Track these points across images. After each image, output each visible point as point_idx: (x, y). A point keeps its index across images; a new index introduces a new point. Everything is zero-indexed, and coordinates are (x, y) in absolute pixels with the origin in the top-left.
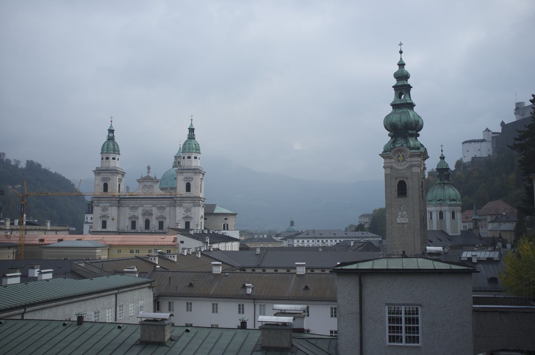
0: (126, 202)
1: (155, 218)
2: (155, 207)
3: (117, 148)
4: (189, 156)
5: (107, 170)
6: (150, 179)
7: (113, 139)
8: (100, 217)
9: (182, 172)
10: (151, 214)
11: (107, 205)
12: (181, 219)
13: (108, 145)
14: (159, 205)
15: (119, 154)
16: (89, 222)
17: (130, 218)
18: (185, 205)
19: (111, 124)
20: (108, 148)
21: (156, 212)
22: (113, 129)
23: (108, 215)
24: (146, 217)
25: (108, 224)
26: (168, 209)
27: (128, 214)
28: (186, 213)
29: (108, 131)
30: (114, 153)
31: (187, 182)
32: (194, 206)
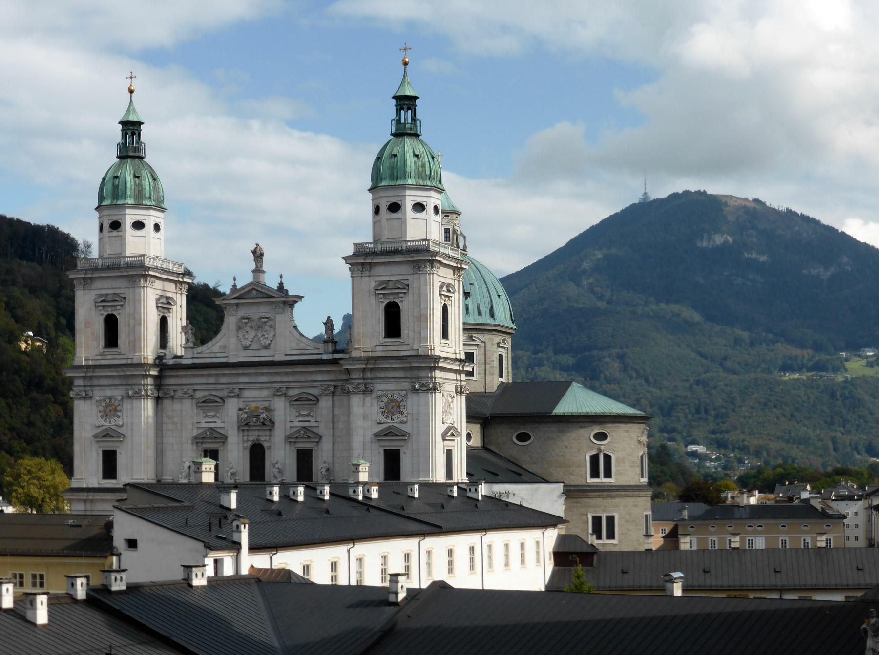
0: (184, 381)
1: (283, 437)
2: (283, 399)
3: (148, 188)
4: (394, 200)
6: (259, 295)
7: (137, 154)
8: (95, 436)
9: (370, 264)
10: (268, 424)
12: (368, 439)
14: (296, 391)
15: (163, 210)
19: (131, 101)
20: (116, 187)
21: (285, 415)
22: (136, 120)
23: (120, 430)
24: (253, 436)
25: (121, 461)
26: (325, 403)
27: (190, 427)
28: (387, 417)
29: (120, 126)
30: (138, 206)
31: (387, 301)
32: (414, 390)
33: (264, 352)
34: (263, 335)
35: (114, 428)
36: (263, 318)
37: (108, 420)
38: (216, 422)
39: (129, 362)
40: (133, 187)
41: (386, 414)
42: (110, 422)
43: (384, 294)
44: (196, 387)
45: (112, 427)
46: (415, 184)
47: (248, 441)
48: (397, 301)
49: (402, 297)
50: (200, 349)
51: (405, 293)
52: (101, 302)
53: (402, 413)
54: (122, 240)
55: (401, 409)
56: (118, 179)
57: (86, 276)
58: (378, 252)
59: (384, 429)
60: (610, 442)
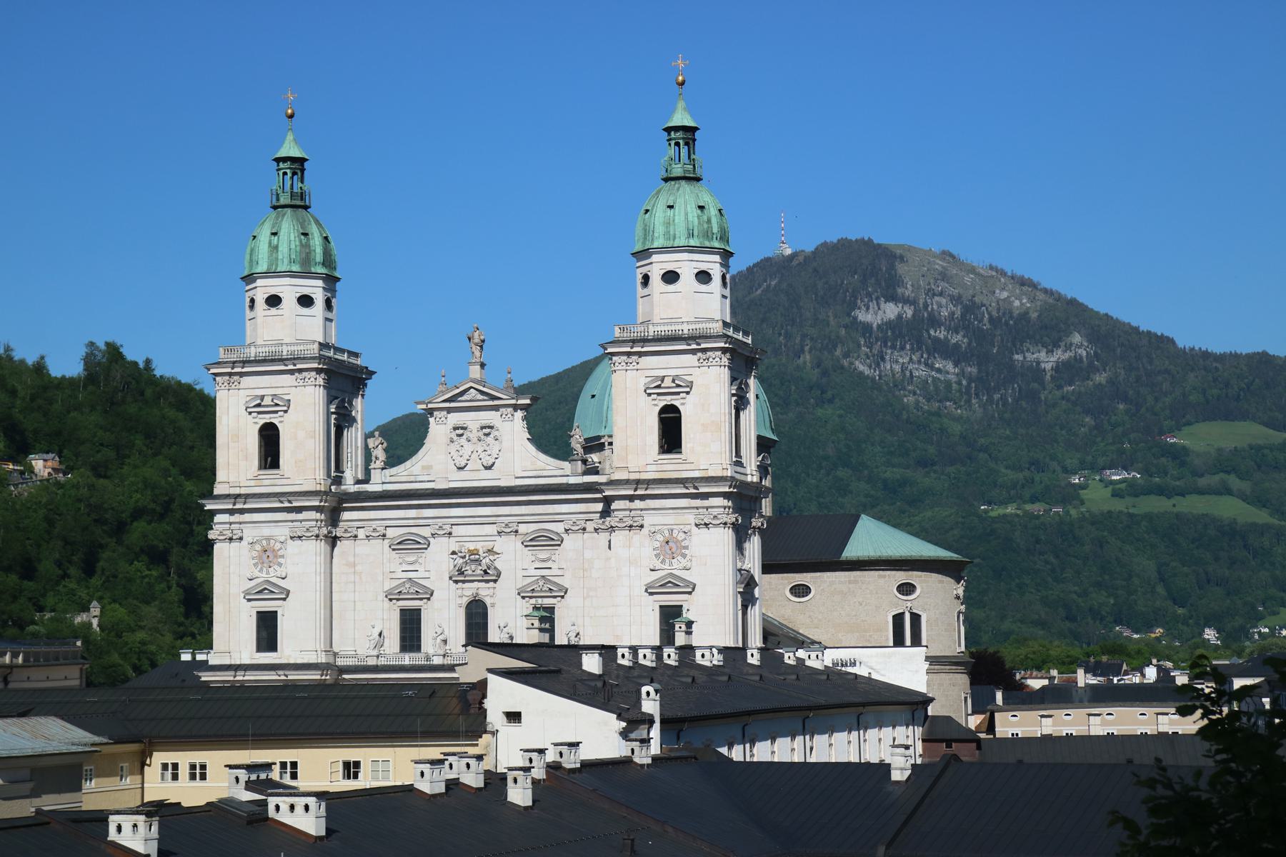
5: (273, 361)
8: (247, 593)
10: (491, 576)
11: (282, 532)
13: (275, 234)
17: (392, 597)
24: (469, 590)
33: (488, 474)
35: (274, 580)
36: (485, 427)
38: (417, 571)
40: (298, 249)
41: (662, 557)
42: (268, 573)
43: (659, 394)
44: (389, 523)
45: (271, 580)
48: (677, 403)
50: (394, 470)
51: (688, 393)
52: (255, 406)
55: (683, 551)
56: (276, 237)
57: (233, 371)
58: (649, 338)
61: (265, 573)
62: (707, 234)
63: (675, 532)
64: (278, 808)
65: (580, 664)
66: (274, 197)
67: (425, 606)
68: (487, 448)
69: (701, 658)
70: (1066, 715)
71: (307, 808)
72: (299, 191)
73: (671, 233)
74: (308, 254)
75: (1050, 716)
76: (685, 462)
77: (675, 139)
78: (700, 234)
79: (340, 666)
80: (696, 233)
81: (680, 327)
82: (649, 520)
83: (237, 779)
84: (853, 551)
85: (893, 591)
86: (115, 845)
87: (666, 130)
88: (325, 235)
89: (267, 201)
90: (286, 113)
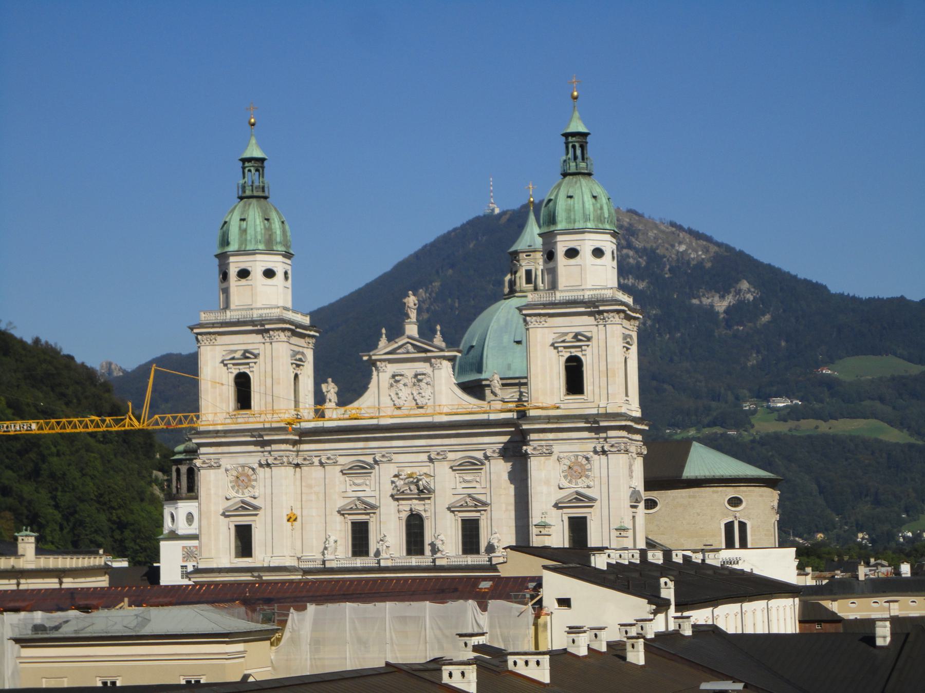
10: (424, 493)
11: (253, 461)
13: (243, 220)
16: (180, 532)
18: (566, 447)
28: (570, 482)
34: (420, 393)
37: (240, 491)
38: (365, 491)
39: (267, 425)
40: (263, 231)
42: (243, 494)
46: (594, 227)
47: (404, 511)
49: (585, 350)
53: (587, 477)
54: (252, 290)
58: (556, 301)
59: (570, 494)
60: (744, 508)
61: (240, 494)
62: (600, 219)
63: (580, 458)
64: (515, 663)
65: (589, 561)
66: (240, 190)
67: (371, 519)
68: (421, 391)
69: (652, 558)
70: (874, 602)
71: (538, 663)
72: (261, 184)
73: (572, 217)
74: (270, 236)
75: (896, 601)
76: (586, 401)
77: (572, 142)
78: (595, 219)
79: (304, 568)
80: (592, 218)
81: (581, 293)
82: (557, 448)
83: (466, 644)
84: (691, 470)
85: (724, 503)
86: (448, 687)
87: (564, 135)
88: (282, 220)
89: (235, 194)
90: (249, 122)
